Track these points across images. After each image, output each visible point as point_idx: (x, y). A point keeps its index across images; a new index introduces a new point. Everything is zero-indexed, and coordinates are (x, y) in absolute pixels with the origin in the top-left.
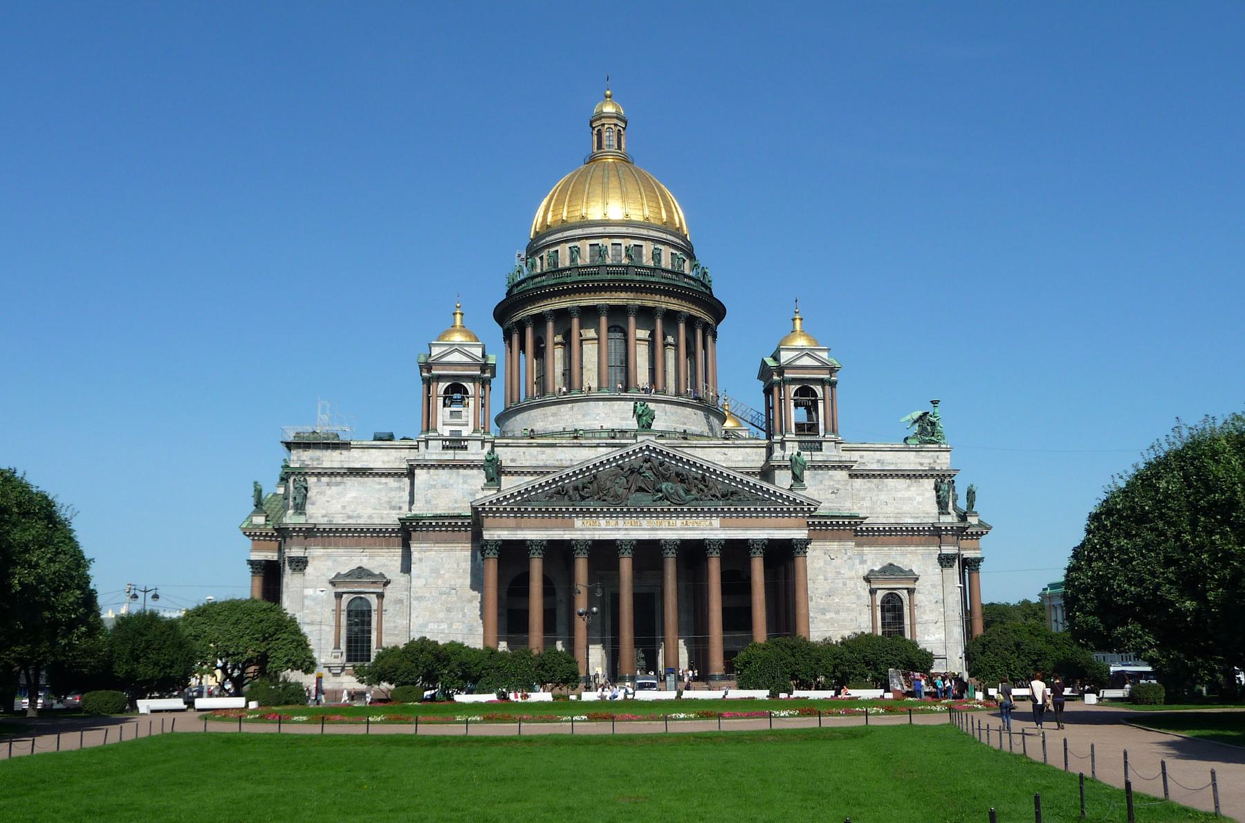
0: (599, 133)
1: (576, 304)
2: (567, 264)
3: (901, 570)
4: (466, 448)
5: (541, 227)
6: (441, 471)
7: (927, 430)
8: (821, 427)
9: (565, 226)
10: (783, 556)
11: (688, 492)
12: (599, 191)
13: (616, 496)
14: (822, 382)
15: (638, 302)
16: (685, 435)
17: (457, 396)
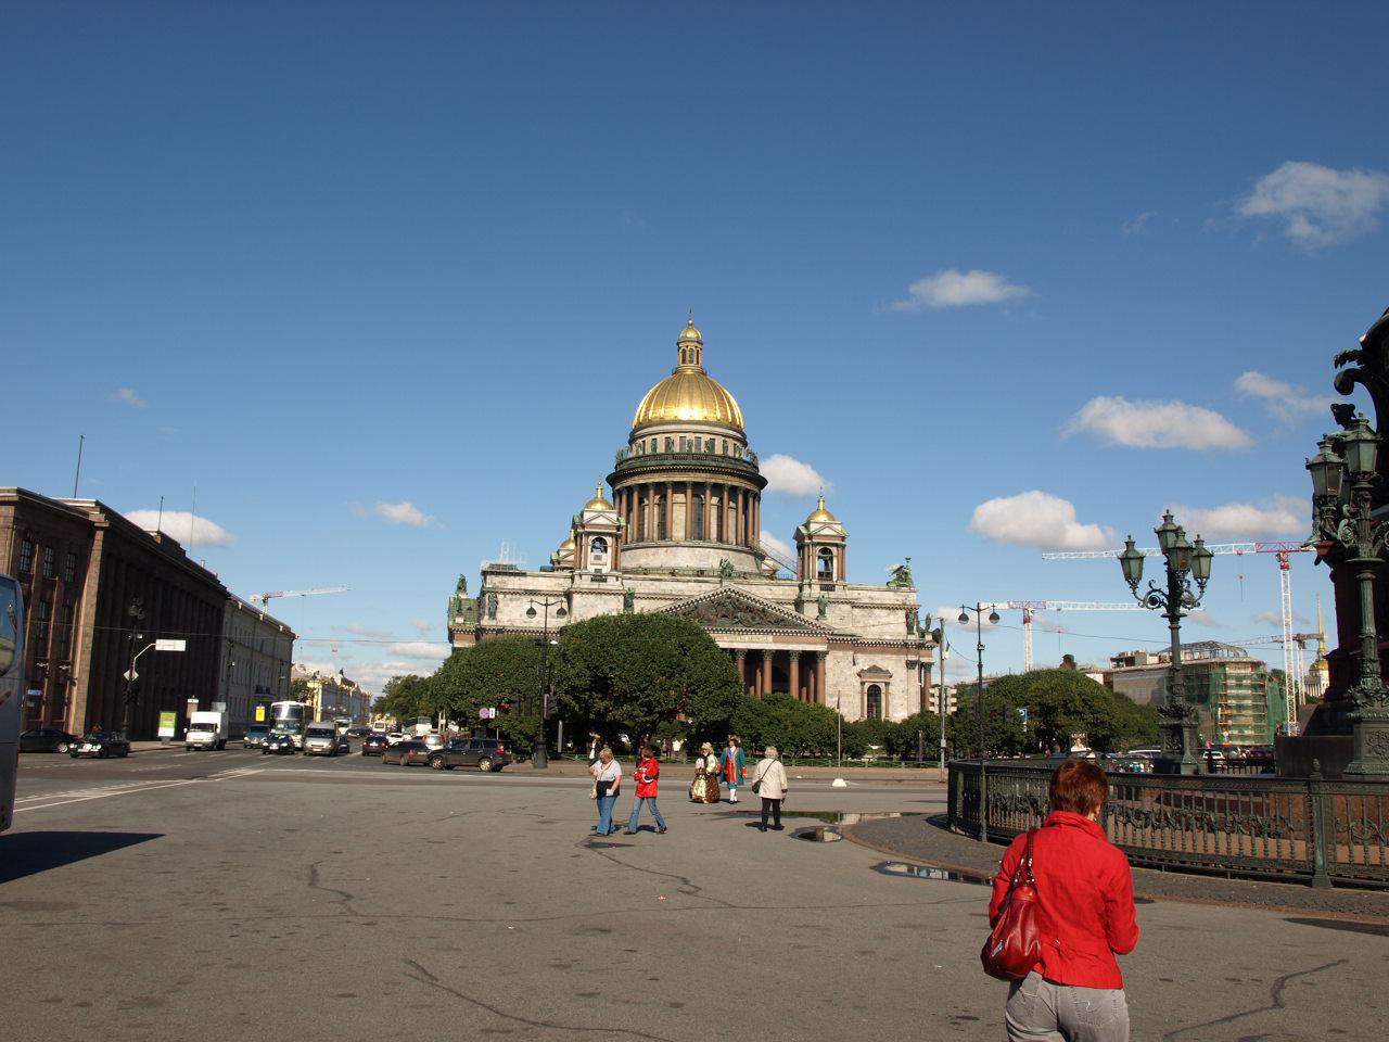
0: (684, 351)
1: (671, 479)
2: (663, 452)
3: (880, 670)
4: (605, 581)
5: (644, 419)
6: (590, 596)
7: (902, 577)
8: (835, 575)
9: (663, 422)
10: (810, 661)
11: (753, 618)
12: (687, 399)
13: (709, 620)
14: (836, 545)
15: (713, 481)
16: (745, 575)
17: (597, 544)
